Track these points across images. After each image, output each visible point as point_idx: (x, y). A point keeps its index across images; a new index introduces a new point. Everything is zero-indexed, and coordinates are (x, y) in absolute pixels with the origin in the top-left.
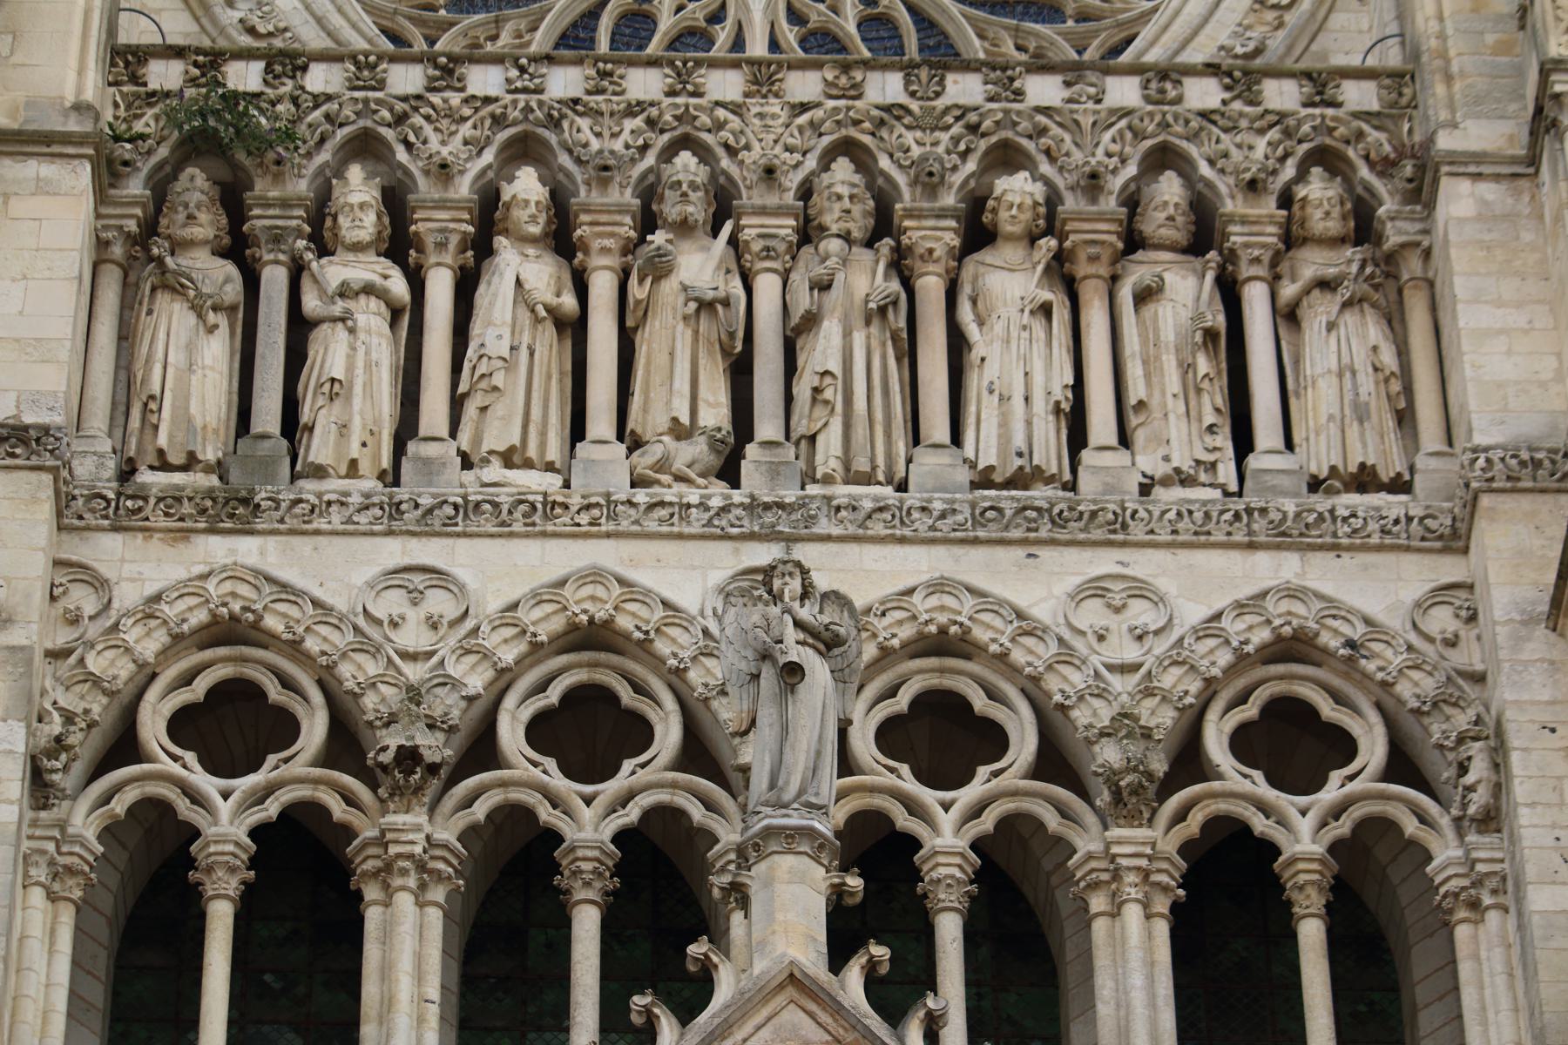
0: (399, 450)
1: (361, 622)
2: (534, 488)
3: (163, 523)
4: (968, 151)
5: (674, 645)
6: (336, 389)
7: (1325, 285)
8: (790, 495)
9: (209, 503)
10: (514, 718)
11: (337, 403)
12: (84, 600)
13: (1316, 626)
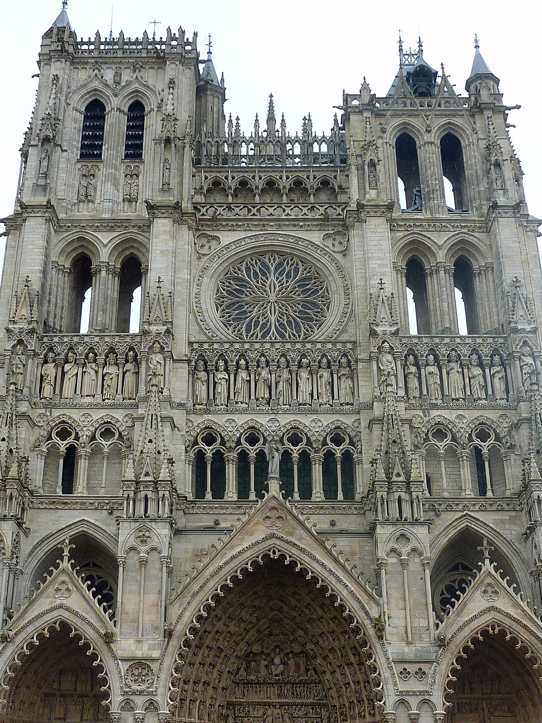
0: (228, 402)
7: (344, 375)
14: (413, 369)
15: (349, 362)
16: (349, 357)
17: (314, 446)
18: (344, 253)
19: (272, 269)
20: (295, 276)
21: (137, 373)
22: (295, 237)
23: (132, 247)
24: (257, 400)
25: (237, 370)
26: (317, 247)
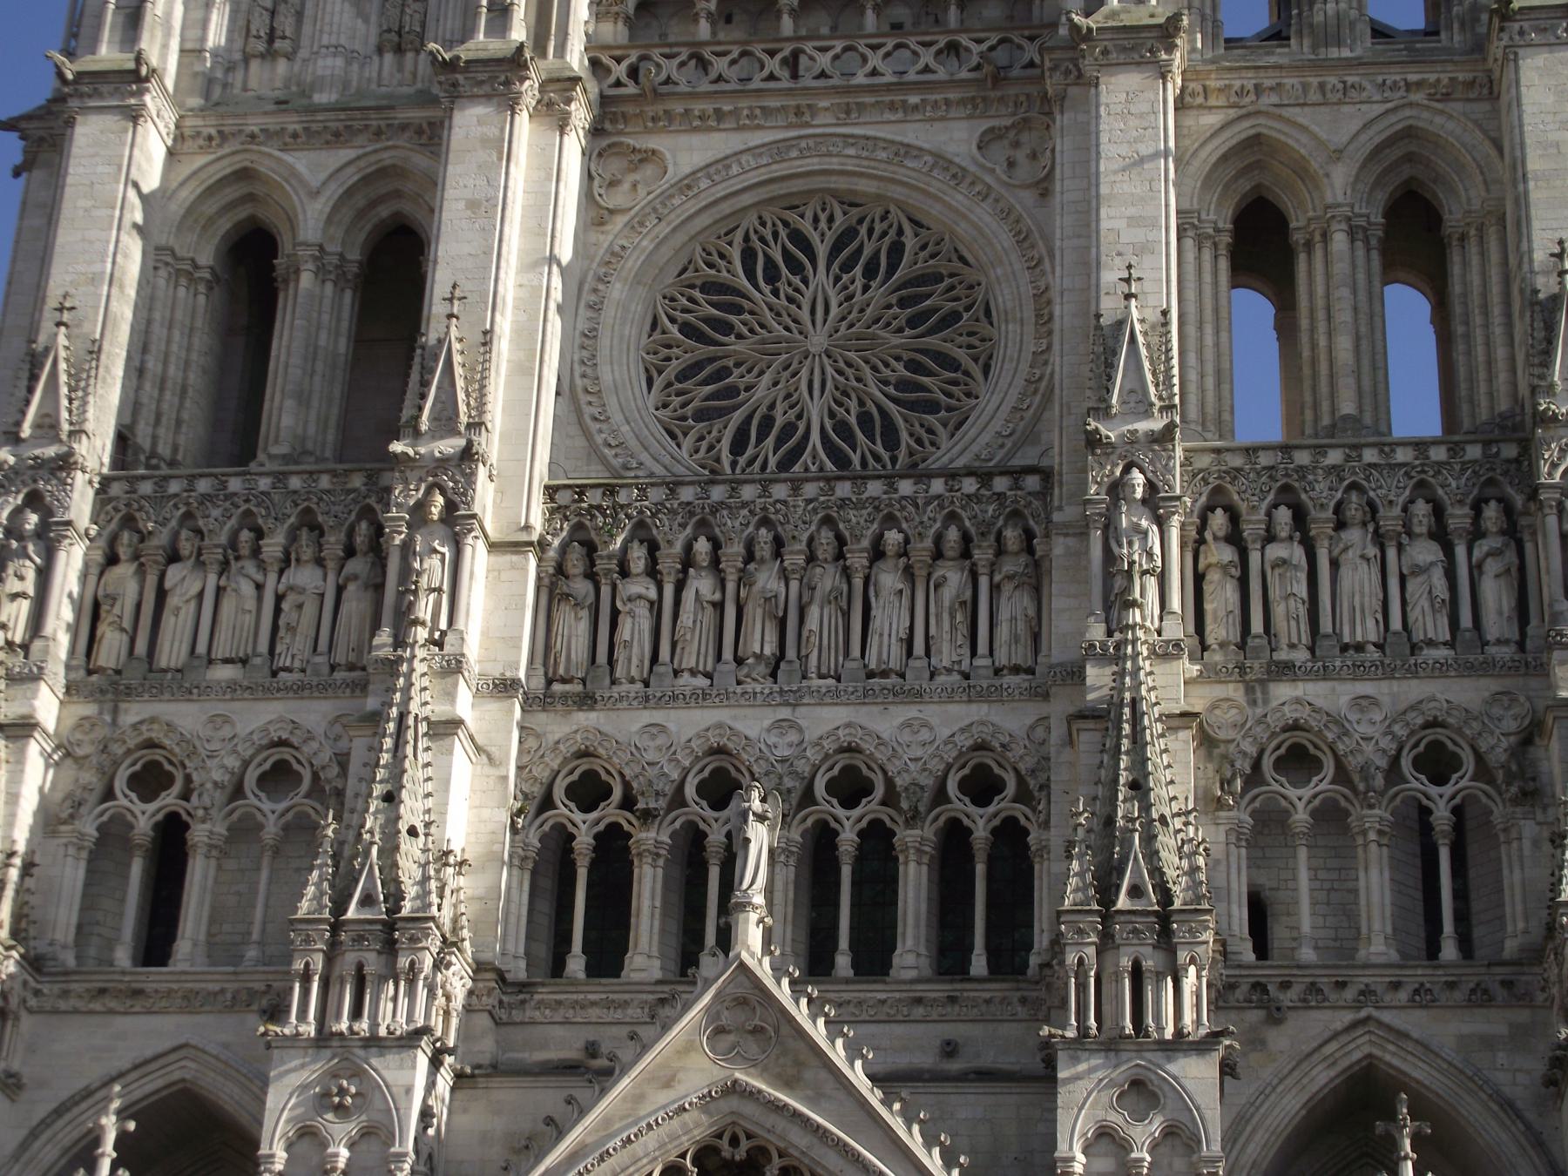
6: (628, 645)
7: (1010, 578)
14: (1227, 554)
15: (1029, 535)
16: (1031, 522)
18: (1044, 188)
19: (822, 251)
20: (892, 269)
21: (379, 588)
22: (892, 142)
23: (397, 194)
24: (739, 661)
25: (685, 571)
26: (958, 175)
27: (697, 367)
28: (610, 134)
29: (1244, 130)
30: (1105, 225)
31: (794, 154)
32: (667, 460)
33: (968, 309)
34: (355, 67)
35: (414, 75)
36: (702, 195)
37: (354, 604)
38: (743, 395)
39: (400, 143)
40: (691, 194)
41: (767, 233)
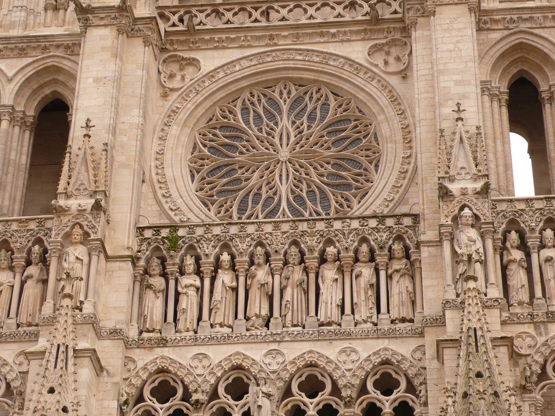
0: (198, 325)
1: (189, 368)
2: (226, 332)
3: (148, 346)
4: (320, 241)
5: (254, 370)
6: (184, 311)
7: (397, 271)
8: (279, 331)
9: (157, 341)
10: (221, 386)
11: (185, 314)
12: (131, 366)
13: (390, 357)
14: (518, 255)
15: (407, 249)
16: (408, 241)
17: (344, 394)
19: (285, 108)
20: (323, 118)
21: (45, 282)
22: (322, 52)
23: (56, 81)
24: (247, 319)
25: (216, 271)
27: (219, 168)
28: (170, 51)
29: (514, 40)
30: (442, 84)
31: (269, 59)
32: (203, 217)
33: (365, 137)
34: (32, 17)
35: (64, 21)
36: (220, 81)
37: (31, 291)
38: (244, 183)
39: (57, 54)
40: (214, 80)
41: (255, 99)
